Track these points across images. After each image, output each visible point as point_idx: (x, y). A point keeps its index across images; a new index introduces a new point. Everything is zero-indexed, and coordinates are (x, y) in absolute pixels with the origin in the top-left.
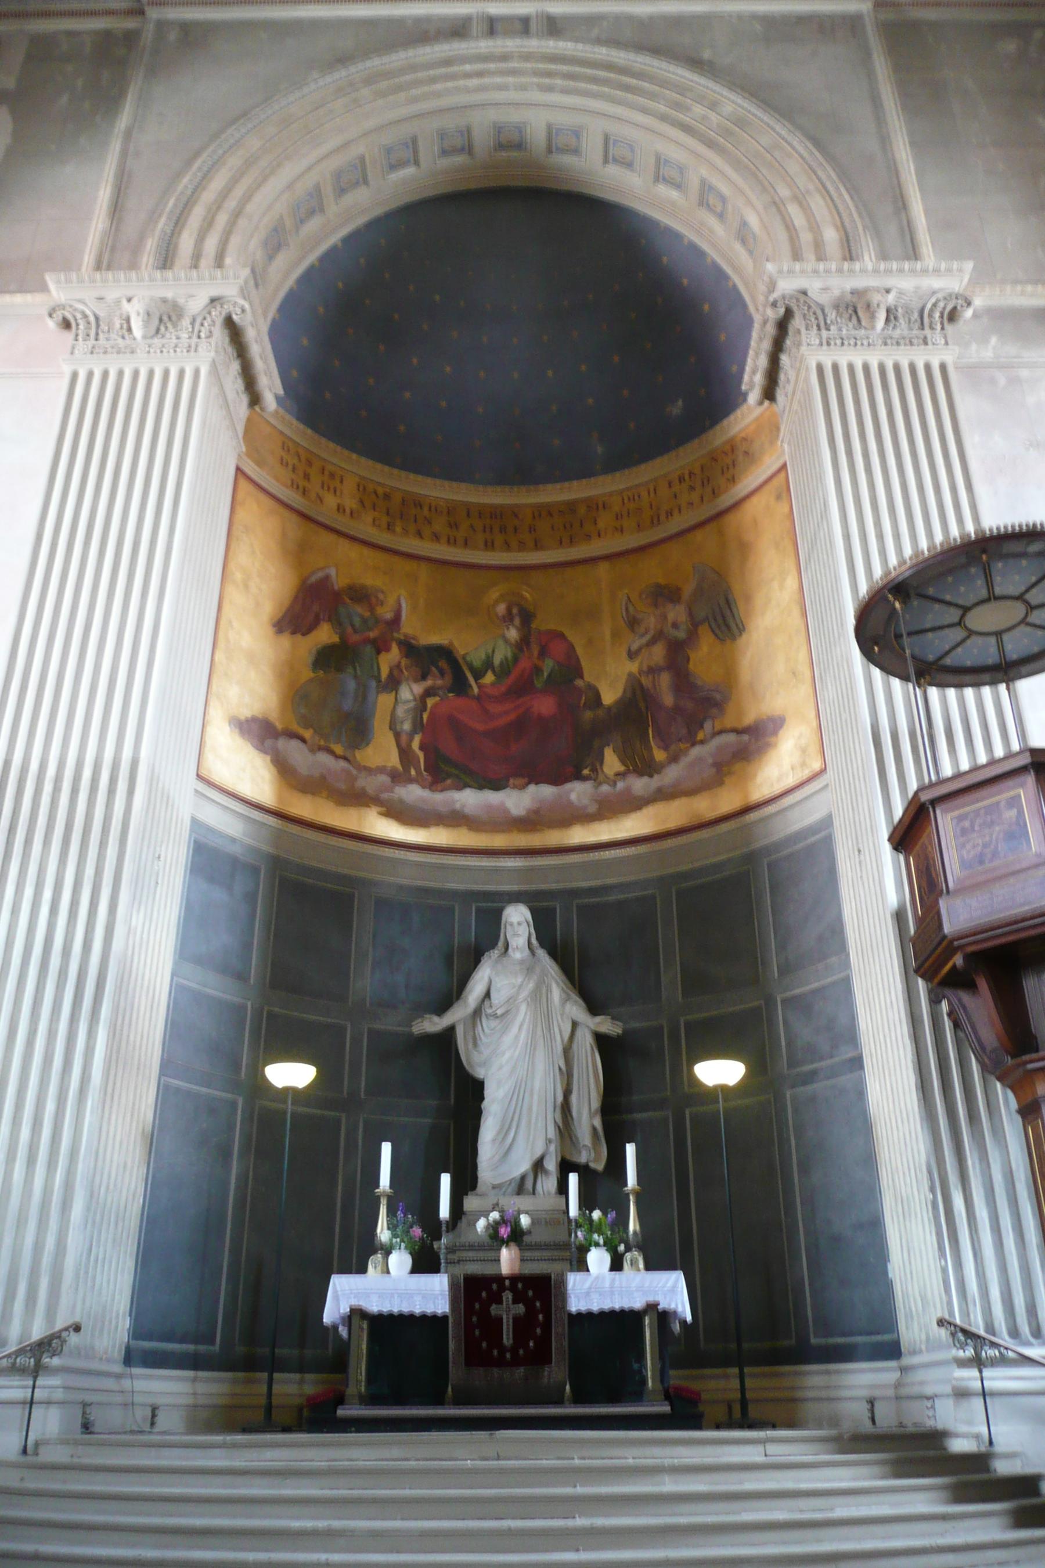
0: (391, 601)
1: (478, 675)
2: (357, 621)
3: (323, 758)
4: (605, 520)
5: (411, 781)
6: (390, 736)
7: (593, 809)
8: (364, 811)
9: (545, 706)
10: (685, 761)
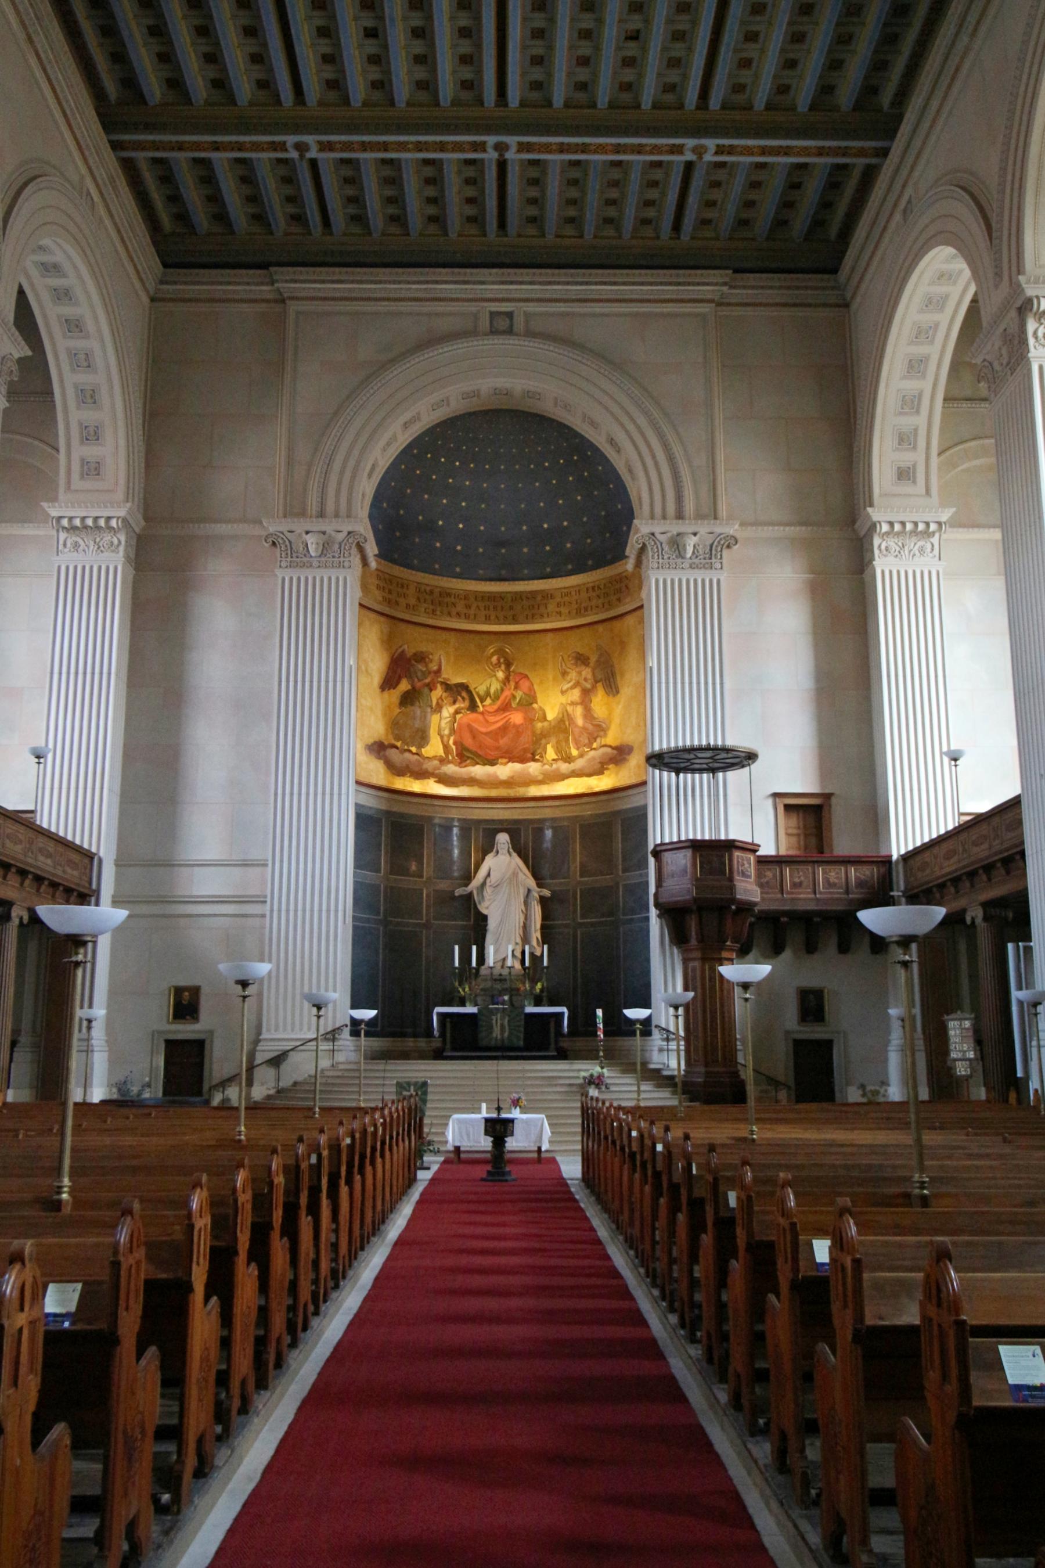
0: (436, 658)
1: (482, 701)
2: (419, 674)
3: (407, 755)
4: (552, 607)
5: (449, 762)
6: (439, 738)
7: (540, 778)
8: (426, 781)
9: (517, 718)
10: (587, 757)
